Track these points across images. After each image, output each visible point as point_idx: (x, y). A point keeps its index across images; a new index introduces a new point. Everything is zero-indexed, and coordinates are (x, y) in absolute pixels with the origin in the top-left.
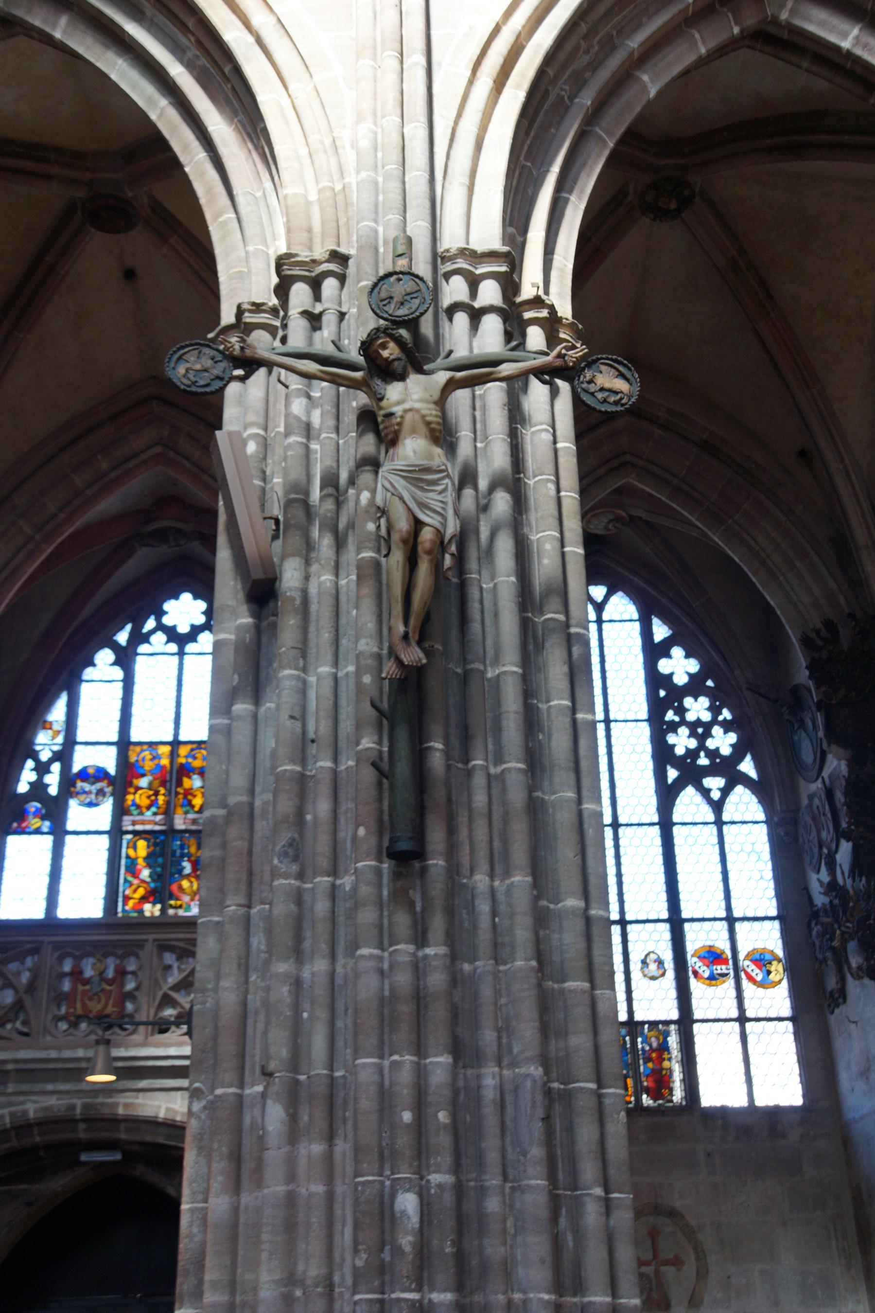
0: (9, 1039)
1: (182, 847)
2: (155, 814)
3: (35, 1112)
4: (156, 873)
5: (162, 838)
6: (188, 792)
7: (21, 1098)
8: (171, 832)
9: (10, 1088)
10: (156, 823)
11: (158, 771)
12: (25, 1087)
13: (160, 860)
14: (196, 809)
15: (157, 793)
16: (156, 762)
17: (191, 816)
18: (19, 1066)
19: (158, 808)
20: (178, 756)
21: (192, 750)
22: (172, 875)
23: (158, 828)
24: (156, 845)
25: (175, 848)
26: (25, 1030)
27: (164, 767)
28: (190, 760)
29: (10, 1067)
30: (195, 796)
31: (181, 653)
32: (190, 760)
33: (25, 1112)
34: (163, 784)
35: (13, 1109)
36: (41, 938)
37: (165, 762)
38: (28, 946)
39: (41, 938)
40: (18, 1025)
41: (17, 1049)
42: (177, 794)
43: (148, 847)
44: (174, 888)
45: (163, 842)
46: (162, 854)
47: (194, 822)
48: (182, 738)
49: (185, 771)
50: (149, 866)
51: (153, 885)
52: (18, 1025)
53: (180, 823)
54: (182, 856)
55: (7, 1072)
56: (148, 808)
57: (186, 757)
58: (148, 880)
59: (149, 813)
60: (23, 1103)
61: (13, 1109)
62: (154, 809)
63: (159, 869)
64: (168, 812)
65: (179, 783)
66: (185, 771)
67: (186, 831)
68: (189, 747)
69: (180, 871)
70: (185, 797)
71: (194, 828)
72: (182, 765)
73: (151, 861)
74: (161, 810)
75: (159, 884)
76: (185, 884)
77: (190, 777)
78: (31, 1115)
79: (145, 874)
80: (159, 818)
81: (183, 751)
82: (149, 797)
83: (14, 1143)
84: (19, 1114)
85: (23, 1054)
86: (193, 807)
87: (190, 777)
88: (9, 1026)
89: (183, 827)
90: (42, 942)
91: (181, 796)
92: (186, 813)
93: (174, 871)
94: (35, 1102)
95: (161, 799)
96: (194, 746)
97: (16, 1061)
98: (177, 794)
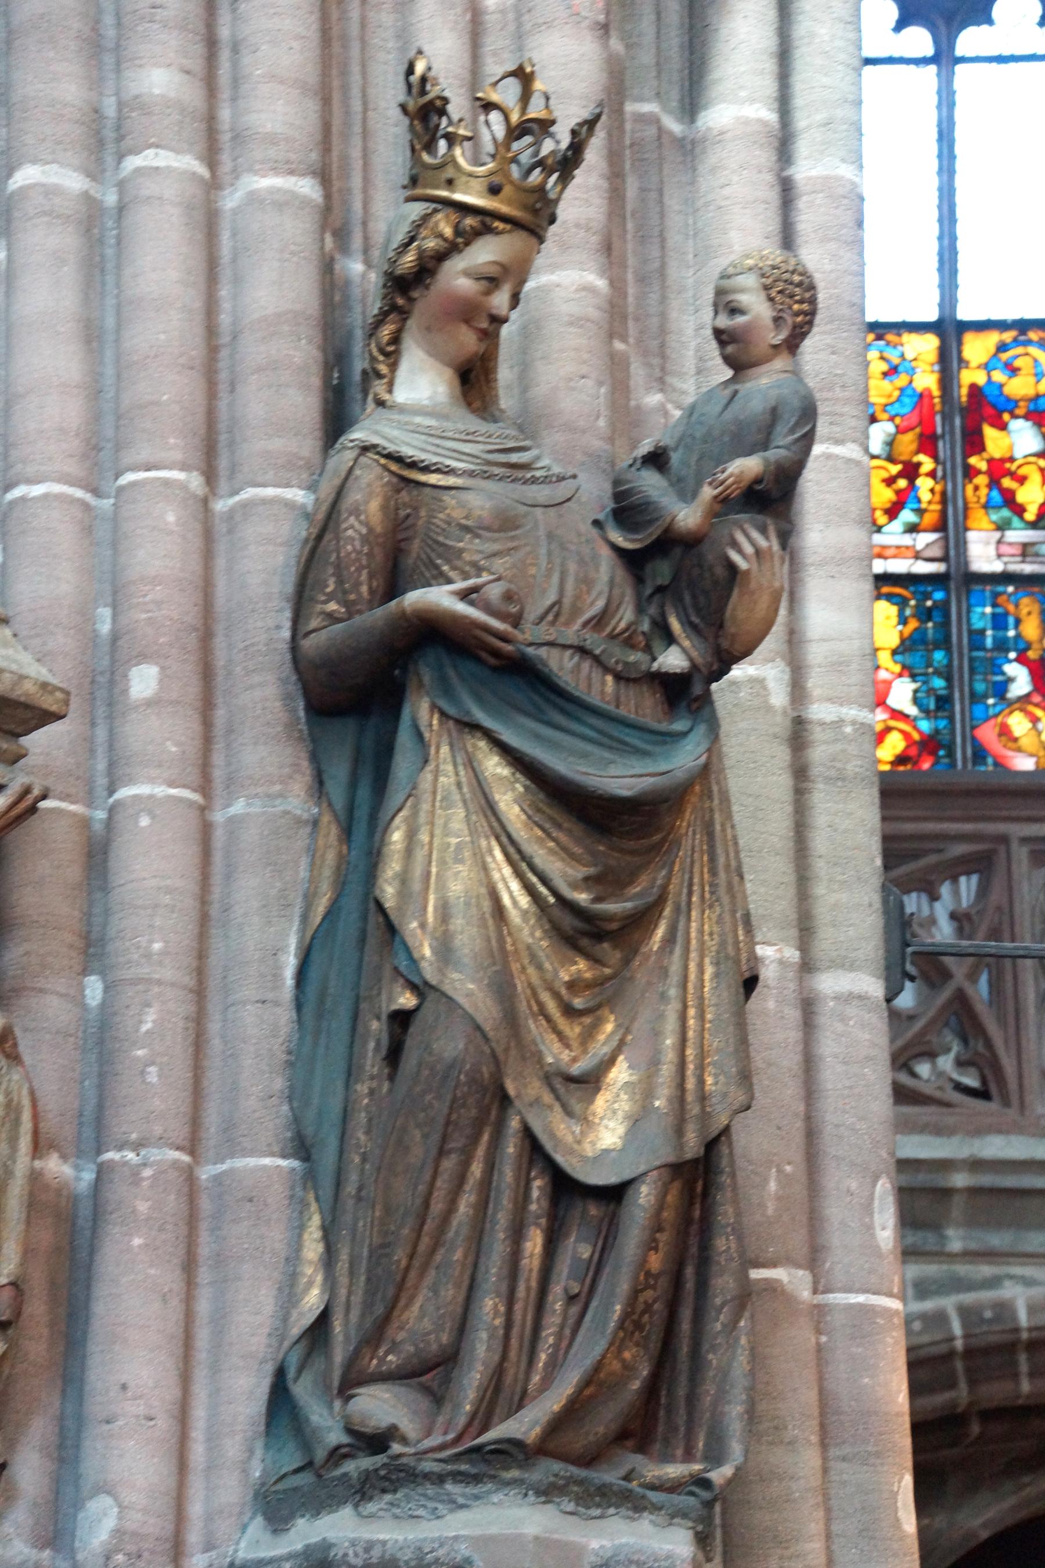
0: (948, 1105)
1: (999, 622)
2: (912, 529)
3: (1032, 1310)
4: (931, 691)
5: (939, 595)
6: (998, 469)
7: (986, 1270)
8: (960, 579)
9: (956, 1240)
10: (917, 556)
11: (907, 406)
12: (997, 1240)
13: (939, 656)
14: (1030, 515)
15: (911, 471)
16: (902, 380)
17: (1018, 535)
18: (987, 1180)
19: (920, 512)
20: (963, 363)
21: (1002, 348)
22: (976, 698)
23: (923, 568)
24: (925, 615)
25: (978, 624)
26: (971, 1081)
27: (923, 397)
28: (998, 376)
29: (960, 1180)
30: (1022, 480)
31: (944, 58)
32: (998, 376)
33: (1004, 1309)
34: (928, 443)
35: (968, 1298)
36: (1001, 828)
37: (927, 380)
38: (959, 849)
39: (1001, 828)
40: (946, 1063)
41: (978, 1132)
42: (970, 473)
43: (903, 620)
44: (988, 734)
45: (944, 607)
46: (944, 643)
47: (1026, 551)
48: (964, 313)
49: (983, 410)
50: (909, 671)
51: (925, 726)
52: (946, 1063)
53: (983, 553)
54: (1002, 646)
55: (947, 1193)
56: (892, 512)
57: (986, 367)
58: (913, 711)
59: (897, 525)
60: (993, 1283)
61: (968, 1298)
62: (907, 516)
63: (939, 683)
64: (950, 525)
65: (975, 443)
66: (983, 410)
67: (1006, 578)
68: (993, 338)
69: (1000, 690)
70: (994, 482)
71: (1028, 568)
72: (974, 388)
73: (915, 659)
74: (929, 519)
75: (942, 724)
76: (1018, 723)
77: (1003, 427)
78: (1023, 1318)
79: (902, 695)
80: (924, 539)
81: (977, 349)
82: (890, 481)
83: (962, 1394)
84: (988, 1314)
85: (996, 1147)
86: (1019, 510)
87: (1003, 427)
88: (924, 1069)
89: (997, 567)
90: (1004, 839)
91: (982, 480)
92: (1001, 527)
93: (980, 687)
94: (1028, 1282)
95: (924, 484)
96: (1008, 336)
97: (976, 1165)
98: (970, 473)
